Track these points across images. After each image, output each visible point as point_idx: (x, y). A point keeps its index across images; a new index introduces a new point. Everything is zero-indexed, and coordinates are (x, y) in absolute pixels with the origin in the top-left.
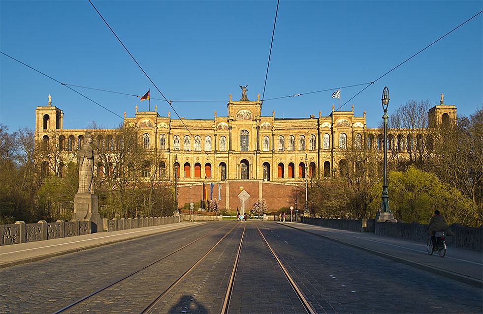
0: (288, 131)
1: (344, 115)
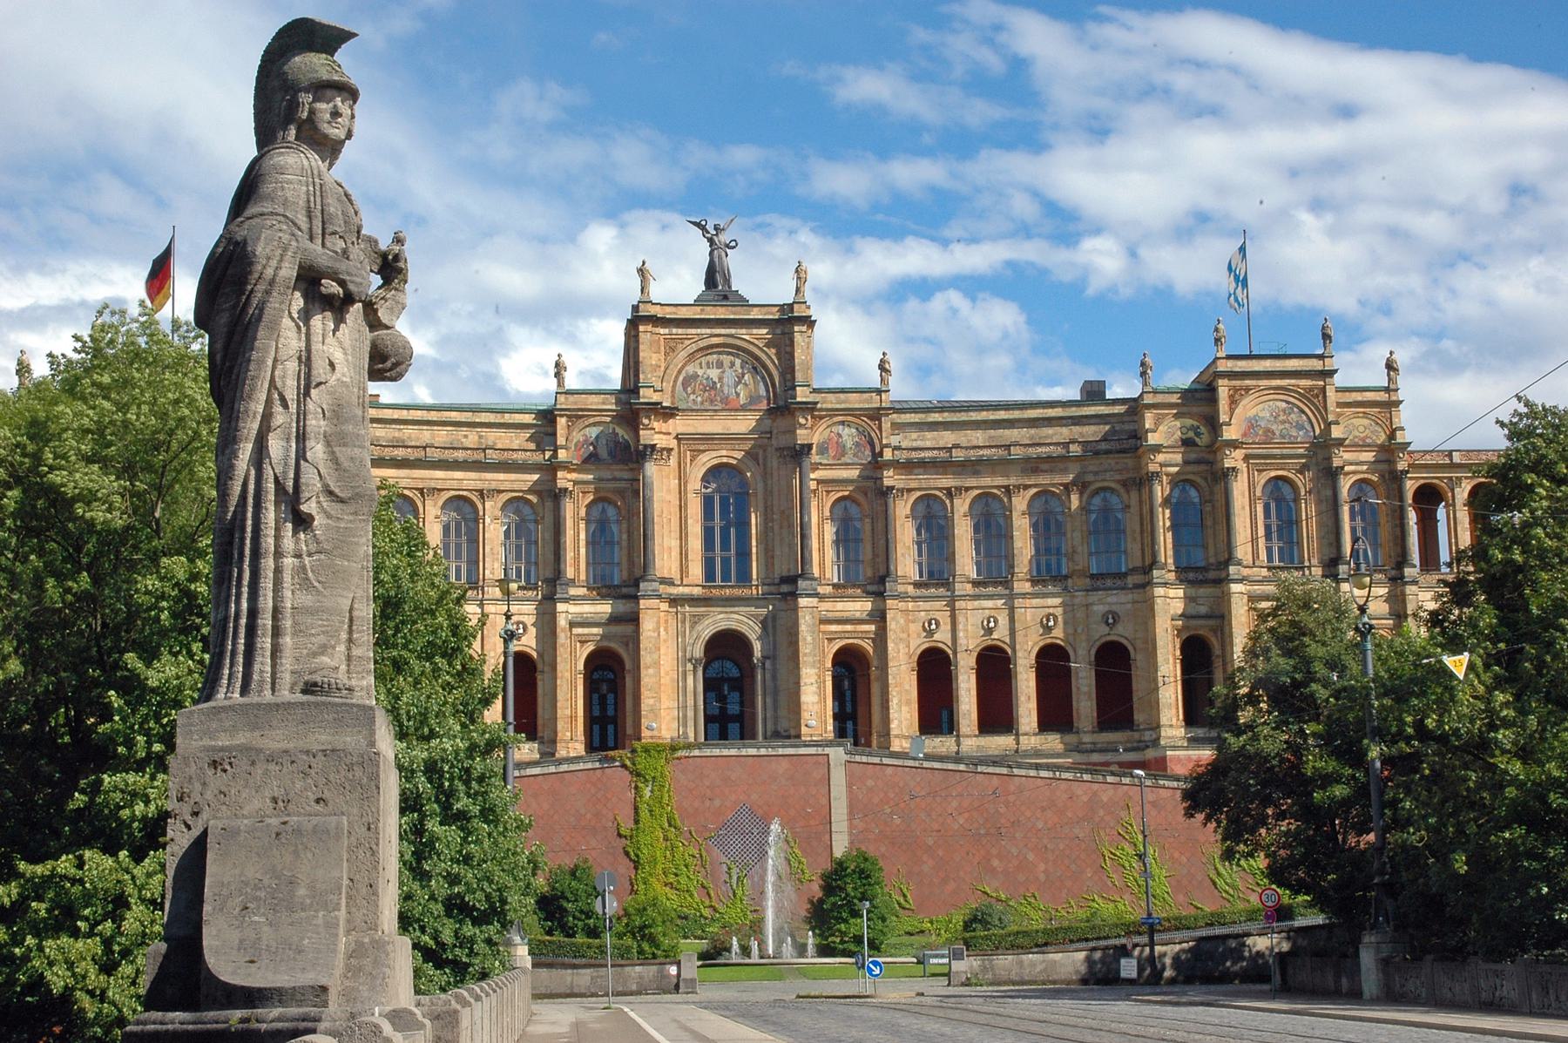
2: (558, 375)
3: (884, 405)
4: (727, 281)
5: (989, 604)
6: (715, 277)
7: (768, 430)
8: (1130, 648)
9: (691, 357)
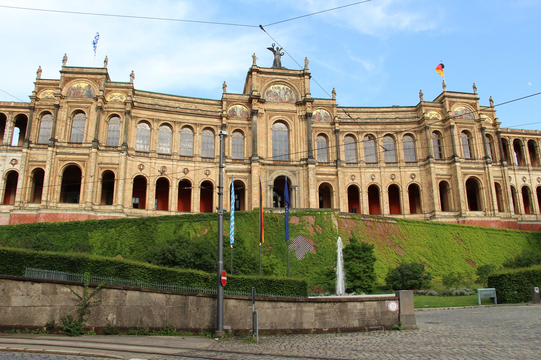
0: (363, 127)
1: (462, 100)
2: (224, 88)
4: (280, 64)
5: (372, 170)
6: (277, 64)
8: (420, 186)
9: (269, 85)
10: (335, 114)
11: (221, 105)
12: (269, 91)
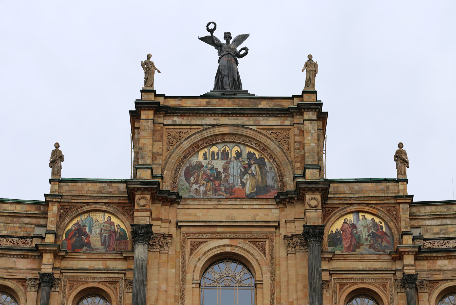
3: (401, 194)
7: (276, 220)
10: (403, 225)
11: (45, 216)
12: (194, 167)
